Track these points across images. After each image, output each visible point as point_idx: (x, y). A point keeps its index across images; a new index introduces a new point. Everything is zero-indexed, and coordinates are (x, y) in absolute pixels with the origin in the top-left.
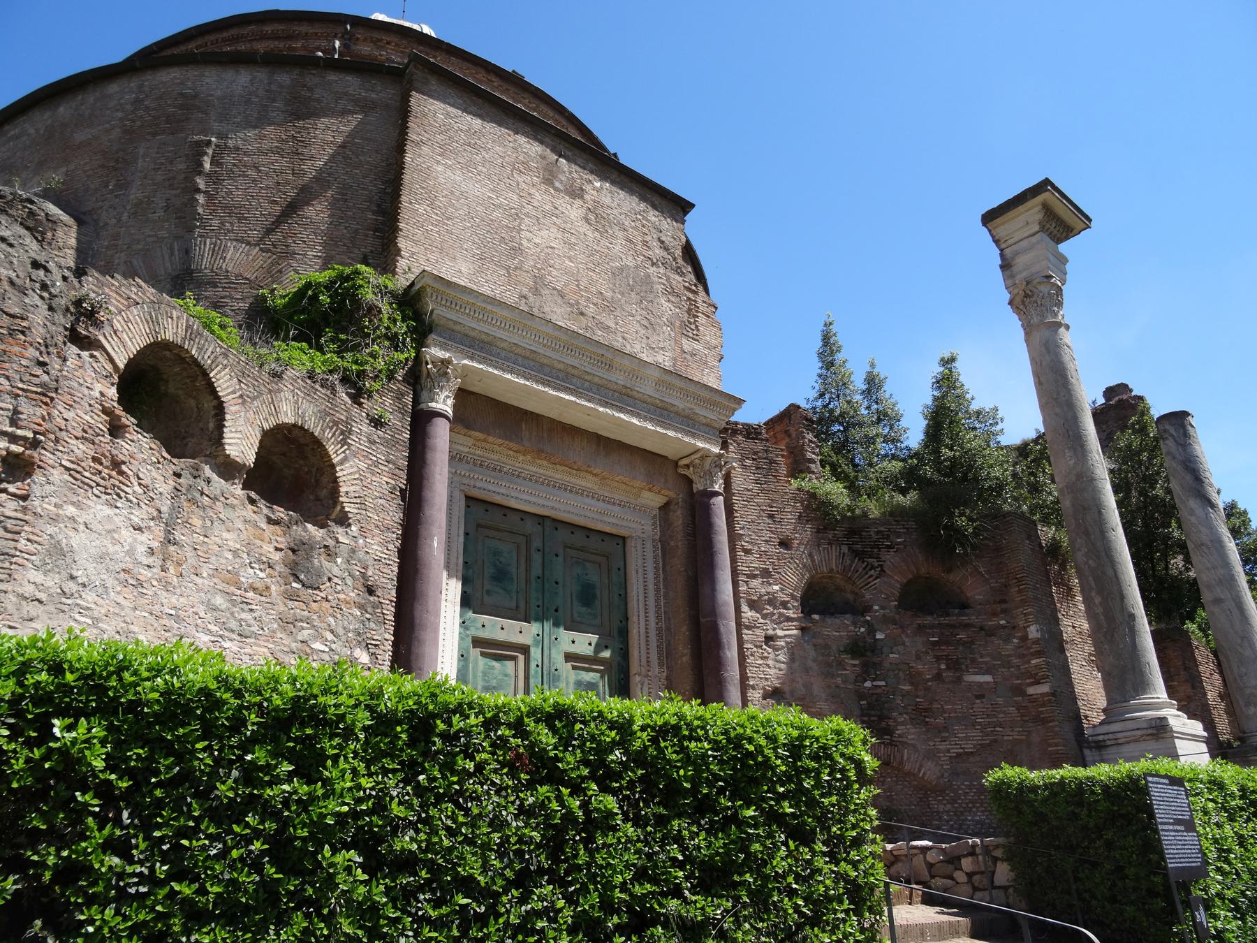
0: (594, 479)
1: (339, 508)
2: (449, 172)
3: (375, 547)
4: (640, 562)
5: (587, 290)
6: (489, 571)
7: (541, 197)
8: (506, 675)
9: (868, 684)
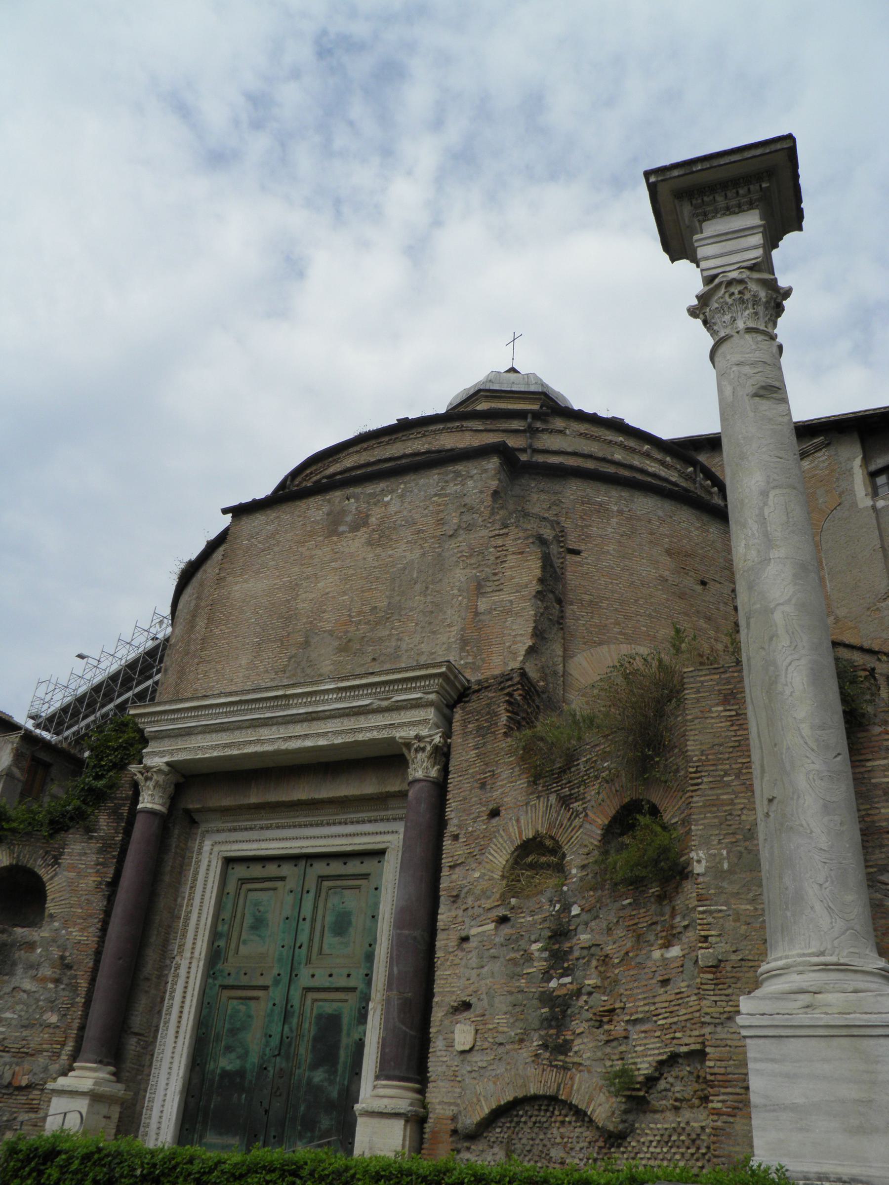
1: (47, 911)
2: (245, 585)
5: (359, 613)
6: (248, 921)
8: (249, 1017)
9: (553, 984)
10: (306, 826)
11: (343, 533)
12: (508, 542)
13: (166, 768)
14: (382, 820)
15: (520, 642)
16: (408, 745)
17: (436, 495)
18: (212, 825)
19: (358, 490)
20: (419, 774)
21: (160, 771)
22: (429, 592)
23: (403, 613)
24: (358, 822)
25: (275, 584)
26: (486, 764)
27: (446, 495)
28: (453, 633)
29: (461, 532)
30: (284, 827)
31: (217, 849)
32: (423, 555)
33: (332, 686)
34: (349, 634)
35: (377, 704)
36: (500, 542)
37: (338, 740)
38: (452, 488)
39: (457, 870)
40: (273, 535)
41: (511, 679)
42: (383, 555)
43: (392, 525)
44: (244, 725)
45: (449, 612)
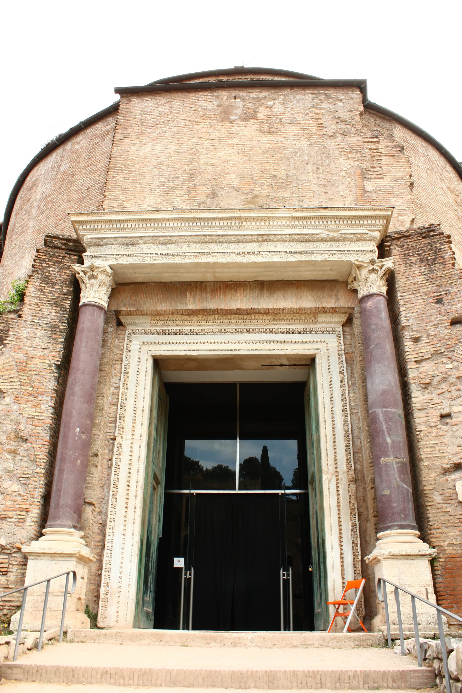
0: (267, 317)
2: (143, 147)
3: (30, 409)
4: (326, 376)
5: (261, 178)
7: (219, 131)
10: (237, 333)
11: (234, 121)
12: (381, 147)
13: (110, 271)
14: (311, 332)
15: (405, 215)
16: (359, 267)
17: (313, 107)
18: (139, 328)
19: (243, 93)
20: (374, 290)
21: (104, 271)
22: (320, 171)
23: (300, 183)
24: (288, 332)
25: (174, 149)
26: (439, 286)
27: (322, 109)
28: (347, 203)
29: (338, 135)
30: (215, 333)
31: (145, 348)
32: (311, 145)
33: (287, 214)
34: (254, 192)
35: (325, 234)
36: (373, 147)
37: (292, 259)
38: (325, 105)
39: (424, 364)
40: (166, 114)
41: (433, 231)
42: (275, 140)
43: (278, 121)
44: (194, 240)
45: (341, 187)
